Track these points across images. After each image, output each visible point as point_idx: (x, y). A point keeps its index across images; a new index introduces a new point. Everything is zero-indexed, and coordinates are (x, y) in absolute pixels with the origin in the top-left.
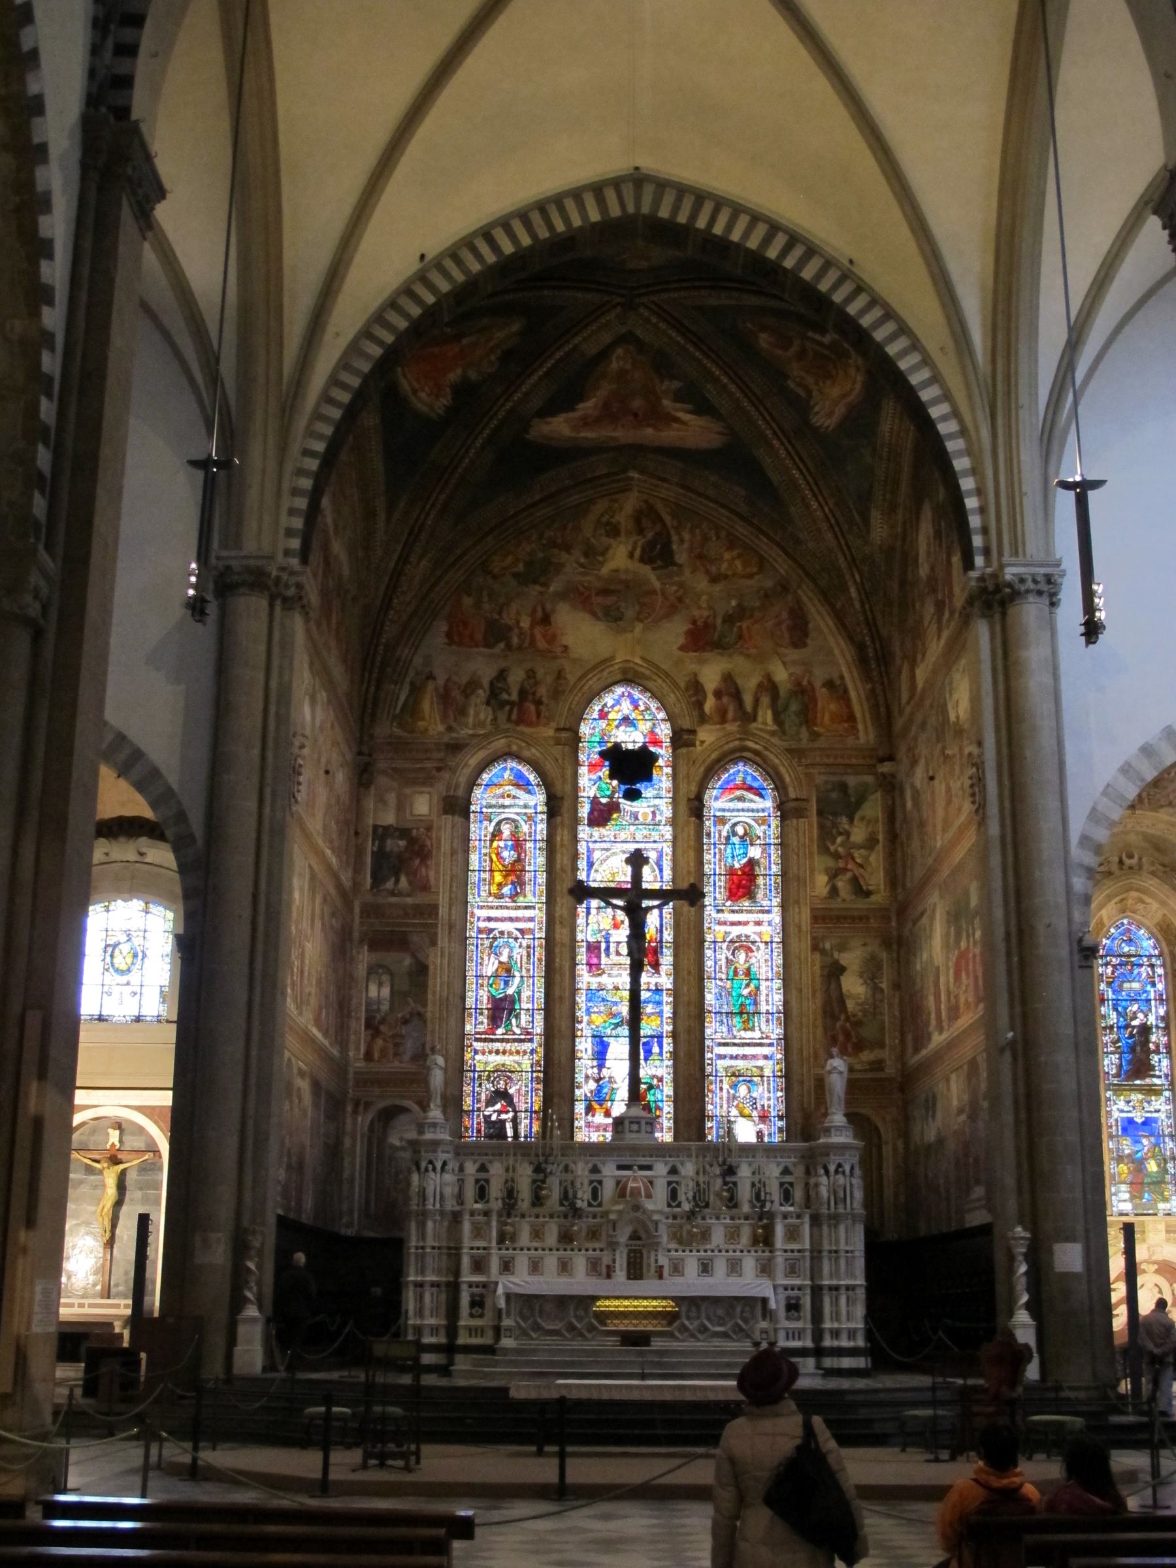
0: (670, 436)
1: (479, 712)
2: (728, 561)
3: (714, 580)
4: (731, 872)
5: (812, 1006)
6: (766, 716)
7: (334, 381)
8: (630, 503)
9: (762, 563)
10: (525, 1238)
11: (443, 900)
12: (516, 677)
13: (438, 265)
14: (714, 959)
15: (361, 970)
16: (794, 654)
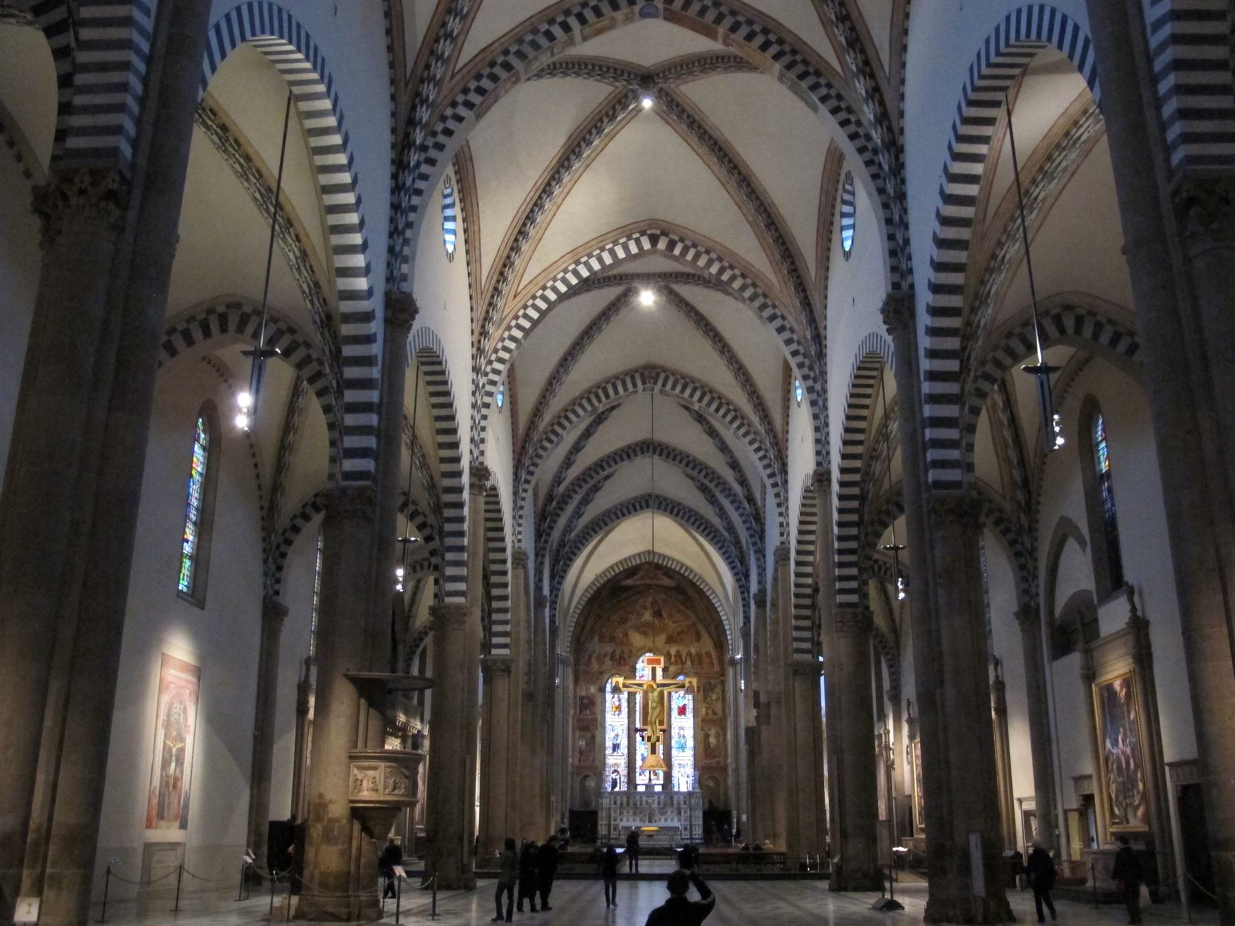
0: (661, 583)
1: (608, 662)
3: (674, 622)
4: (679, 708)
5: (701, 748)
6: (689, 663)
8: (650, 599)
10: (625, 813)
11: (599, 717)
12: (618, 652)
13: (600, 576)
14: (674, 732)
15: (577, 737)
16: (696, 644)
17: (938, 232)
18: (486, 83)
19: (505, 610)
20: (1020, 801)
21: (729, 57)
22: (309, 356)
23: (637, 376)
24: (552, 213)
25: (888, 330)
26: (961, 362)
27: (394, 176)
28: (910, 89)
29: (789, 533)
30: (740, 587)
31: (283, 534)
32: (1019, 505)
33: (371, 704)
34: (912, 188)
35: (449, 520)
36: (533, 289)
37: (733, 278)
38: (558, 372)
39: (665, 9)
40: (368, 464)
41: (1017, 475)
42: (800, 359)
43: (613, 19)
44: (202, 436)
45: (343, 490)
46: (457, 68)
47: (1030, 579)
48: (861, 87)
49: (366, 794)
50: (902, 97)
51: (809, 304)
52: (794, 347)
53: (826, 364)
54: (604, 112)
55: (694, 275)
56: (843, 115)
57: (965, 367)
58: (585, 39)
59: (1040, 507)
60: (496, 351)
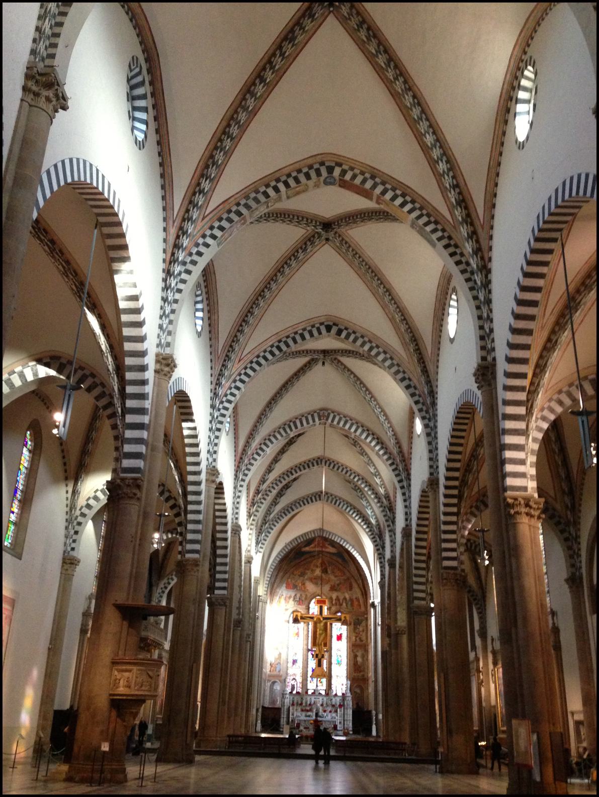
0: (327, 550)
2: (338, 573)
3: (336, 576)
5: (352, 664)
6: (344, 604)
7: (272, 565)
8: (320, 561)
9: (344, 574)
12: (298, 596)
13: (288, 544)
16: (349, 592)
17: (512, 324)
18: (225, 224)
19: (225, 564)
20: (573, 714)
21: (380, 212)
22: (104, 392)
23: (316, 415)
24: (265, 309)
25: (478, 387)
26: (527, 409)
27: (165, 280)
28: (496, 233)
29: (411, 520)
30: (379, 554)
31: (80, 510)
32: (567, 507)
33: (131, 626)
34: (495, 296)
35: (192, 503)
36: (250, 357)
37: (378, 354)
38: (265, 411)
39: (340, 180)
40: (140, 463)
41: (565, 486)
42: (420, 406)
43: (306, 185)
44: (29, 443)
45: (123, 479)
46: (207, 213)
47: (575, 557)
48: (464, 231)
49: (121, 690)
50: (491, 238)
51: (427, 371)
52: (416, 398)
53: (437, 410)
54: (299, 246)
55: (353, 351)
56: (452, 250)
57: (530, 412)
58: (288, 198)
59: (582, 508)
60: (226, 395)
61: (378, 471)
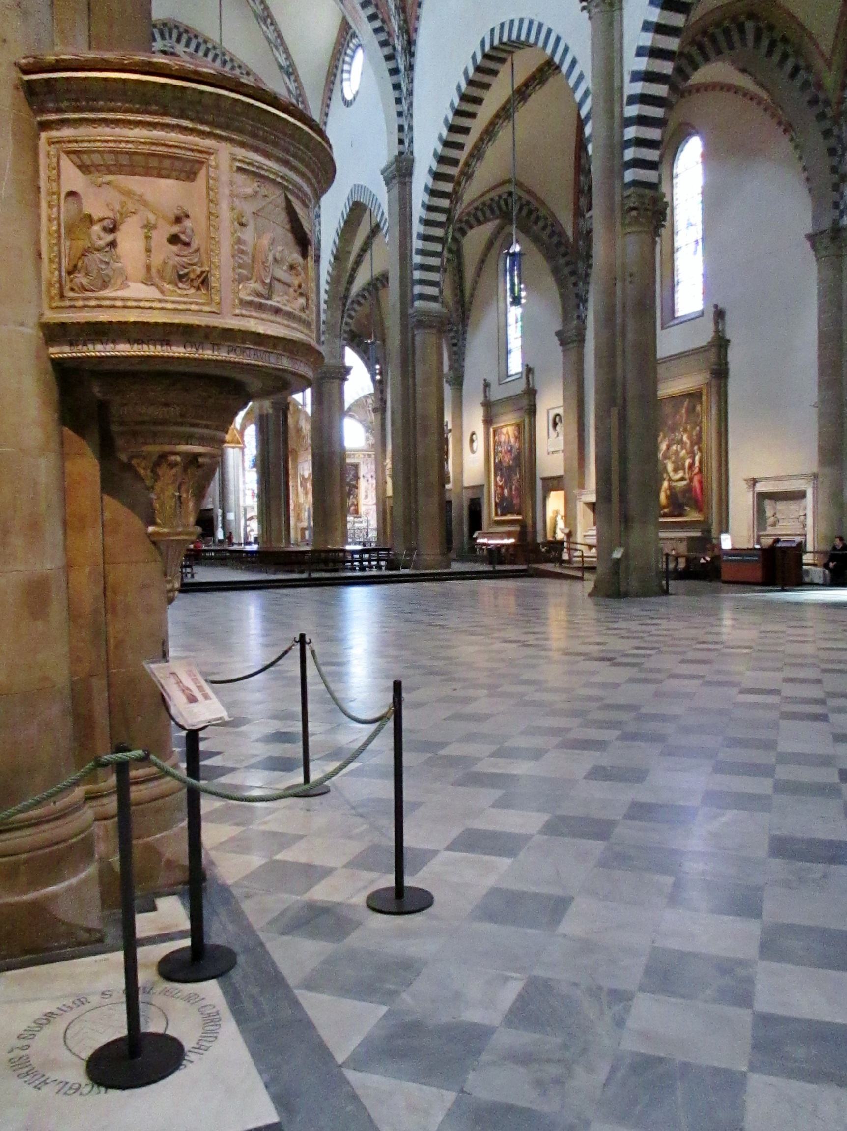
29: (411, 141)
61: (292, 65)
